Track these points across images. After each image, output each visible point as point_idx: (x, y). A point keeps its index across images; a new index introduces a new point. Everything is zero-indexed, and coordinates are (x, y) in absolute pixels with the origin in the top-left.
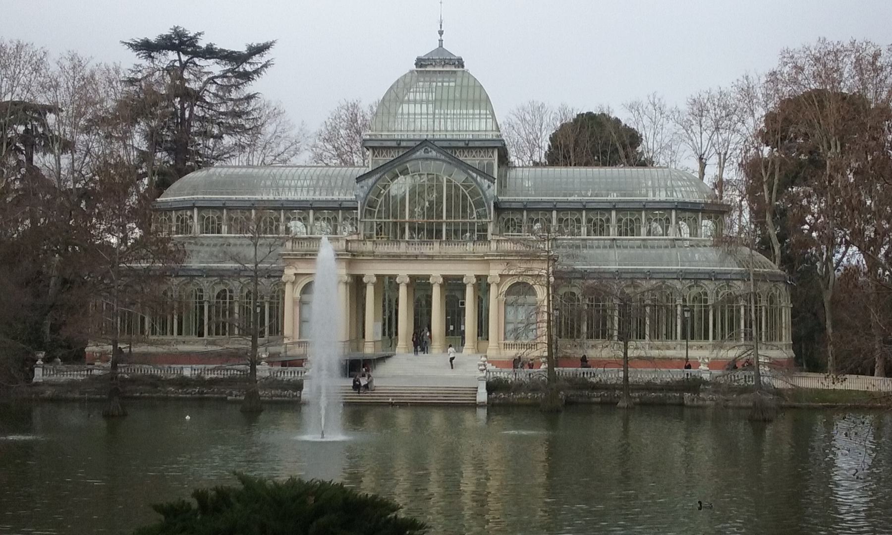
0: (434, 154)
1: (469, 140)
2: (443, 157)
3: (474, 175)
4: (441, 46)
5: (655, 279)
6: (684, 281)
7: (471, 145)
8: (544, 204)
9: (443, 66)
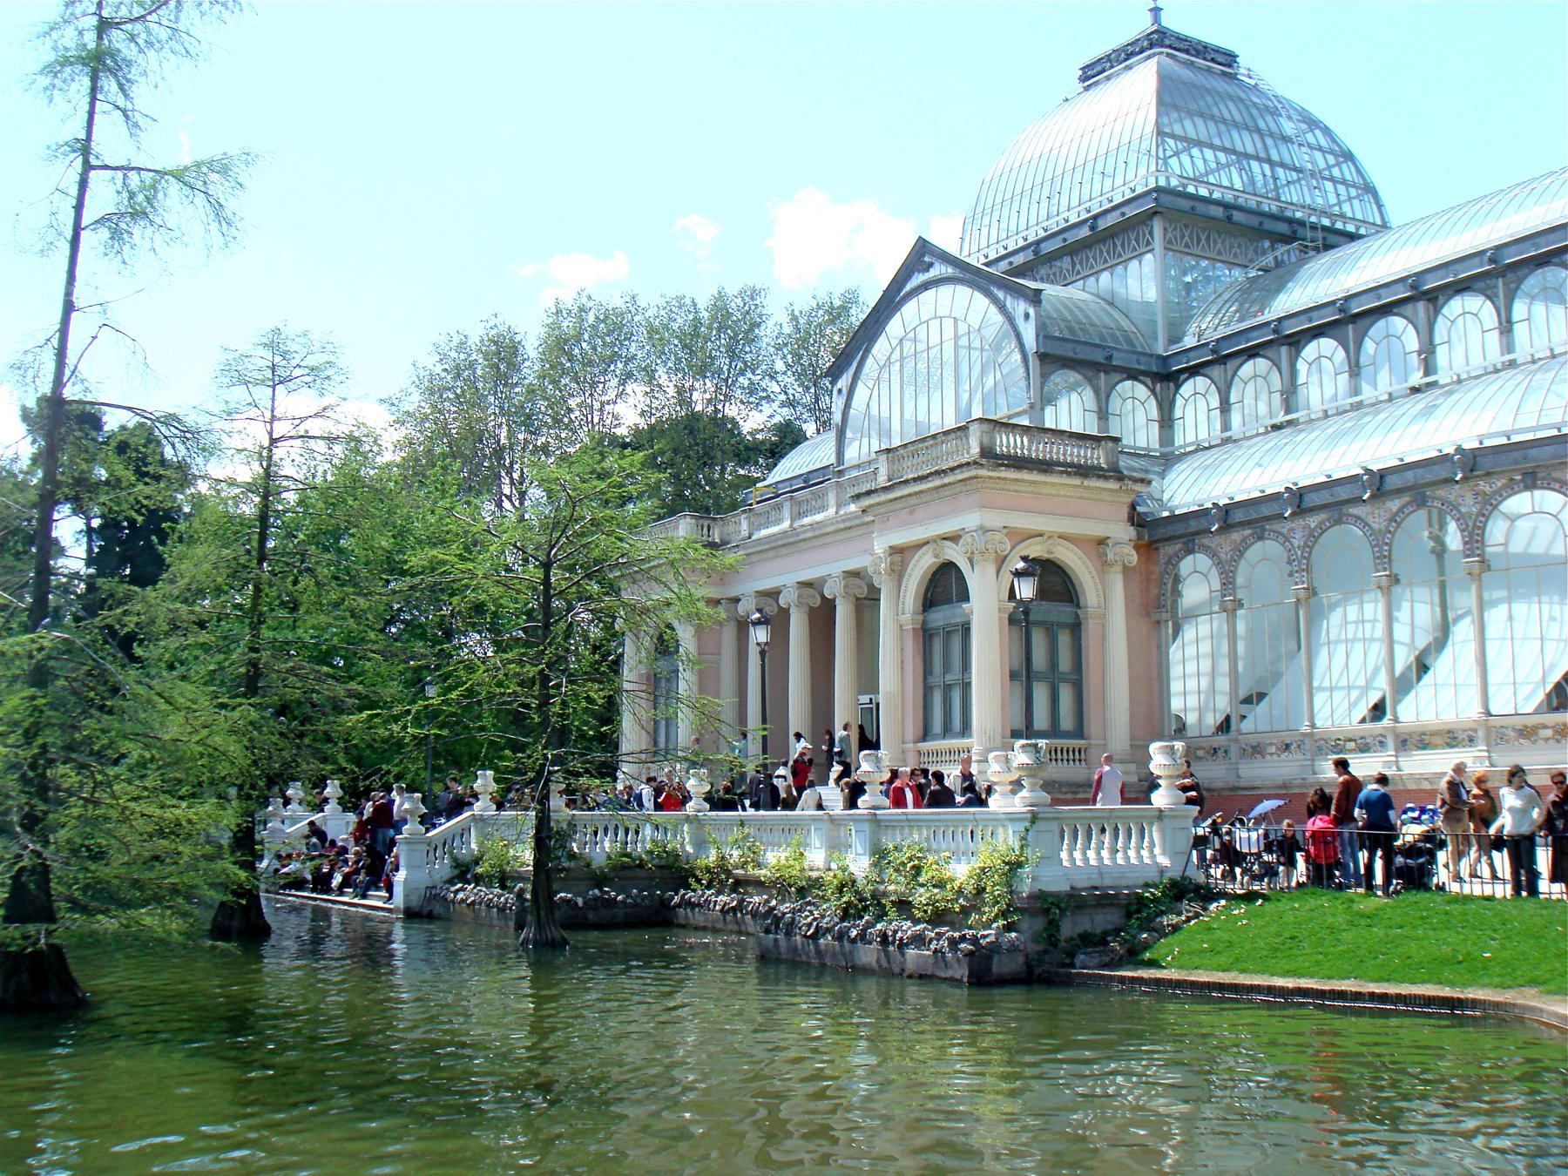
0: (939, 270)
1: (1095, 217)
2: (950, 270)
3: (1000, 294)
4: (1156, 20)
5: (1398, 492)
6: (1483, 486)
7: (1103, 224)
8: (1256, 333)
9: (1126, 60)
